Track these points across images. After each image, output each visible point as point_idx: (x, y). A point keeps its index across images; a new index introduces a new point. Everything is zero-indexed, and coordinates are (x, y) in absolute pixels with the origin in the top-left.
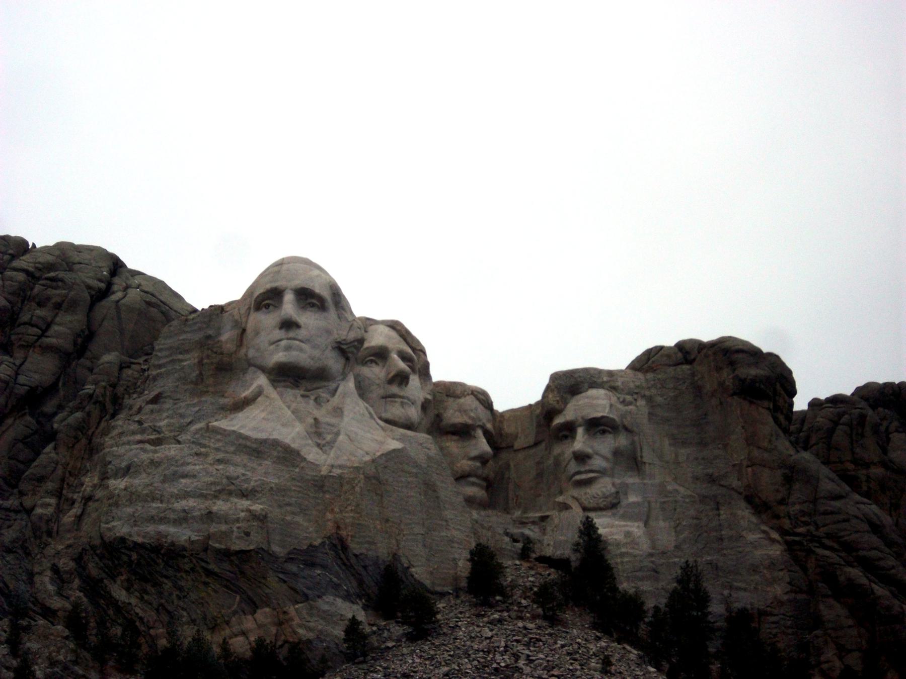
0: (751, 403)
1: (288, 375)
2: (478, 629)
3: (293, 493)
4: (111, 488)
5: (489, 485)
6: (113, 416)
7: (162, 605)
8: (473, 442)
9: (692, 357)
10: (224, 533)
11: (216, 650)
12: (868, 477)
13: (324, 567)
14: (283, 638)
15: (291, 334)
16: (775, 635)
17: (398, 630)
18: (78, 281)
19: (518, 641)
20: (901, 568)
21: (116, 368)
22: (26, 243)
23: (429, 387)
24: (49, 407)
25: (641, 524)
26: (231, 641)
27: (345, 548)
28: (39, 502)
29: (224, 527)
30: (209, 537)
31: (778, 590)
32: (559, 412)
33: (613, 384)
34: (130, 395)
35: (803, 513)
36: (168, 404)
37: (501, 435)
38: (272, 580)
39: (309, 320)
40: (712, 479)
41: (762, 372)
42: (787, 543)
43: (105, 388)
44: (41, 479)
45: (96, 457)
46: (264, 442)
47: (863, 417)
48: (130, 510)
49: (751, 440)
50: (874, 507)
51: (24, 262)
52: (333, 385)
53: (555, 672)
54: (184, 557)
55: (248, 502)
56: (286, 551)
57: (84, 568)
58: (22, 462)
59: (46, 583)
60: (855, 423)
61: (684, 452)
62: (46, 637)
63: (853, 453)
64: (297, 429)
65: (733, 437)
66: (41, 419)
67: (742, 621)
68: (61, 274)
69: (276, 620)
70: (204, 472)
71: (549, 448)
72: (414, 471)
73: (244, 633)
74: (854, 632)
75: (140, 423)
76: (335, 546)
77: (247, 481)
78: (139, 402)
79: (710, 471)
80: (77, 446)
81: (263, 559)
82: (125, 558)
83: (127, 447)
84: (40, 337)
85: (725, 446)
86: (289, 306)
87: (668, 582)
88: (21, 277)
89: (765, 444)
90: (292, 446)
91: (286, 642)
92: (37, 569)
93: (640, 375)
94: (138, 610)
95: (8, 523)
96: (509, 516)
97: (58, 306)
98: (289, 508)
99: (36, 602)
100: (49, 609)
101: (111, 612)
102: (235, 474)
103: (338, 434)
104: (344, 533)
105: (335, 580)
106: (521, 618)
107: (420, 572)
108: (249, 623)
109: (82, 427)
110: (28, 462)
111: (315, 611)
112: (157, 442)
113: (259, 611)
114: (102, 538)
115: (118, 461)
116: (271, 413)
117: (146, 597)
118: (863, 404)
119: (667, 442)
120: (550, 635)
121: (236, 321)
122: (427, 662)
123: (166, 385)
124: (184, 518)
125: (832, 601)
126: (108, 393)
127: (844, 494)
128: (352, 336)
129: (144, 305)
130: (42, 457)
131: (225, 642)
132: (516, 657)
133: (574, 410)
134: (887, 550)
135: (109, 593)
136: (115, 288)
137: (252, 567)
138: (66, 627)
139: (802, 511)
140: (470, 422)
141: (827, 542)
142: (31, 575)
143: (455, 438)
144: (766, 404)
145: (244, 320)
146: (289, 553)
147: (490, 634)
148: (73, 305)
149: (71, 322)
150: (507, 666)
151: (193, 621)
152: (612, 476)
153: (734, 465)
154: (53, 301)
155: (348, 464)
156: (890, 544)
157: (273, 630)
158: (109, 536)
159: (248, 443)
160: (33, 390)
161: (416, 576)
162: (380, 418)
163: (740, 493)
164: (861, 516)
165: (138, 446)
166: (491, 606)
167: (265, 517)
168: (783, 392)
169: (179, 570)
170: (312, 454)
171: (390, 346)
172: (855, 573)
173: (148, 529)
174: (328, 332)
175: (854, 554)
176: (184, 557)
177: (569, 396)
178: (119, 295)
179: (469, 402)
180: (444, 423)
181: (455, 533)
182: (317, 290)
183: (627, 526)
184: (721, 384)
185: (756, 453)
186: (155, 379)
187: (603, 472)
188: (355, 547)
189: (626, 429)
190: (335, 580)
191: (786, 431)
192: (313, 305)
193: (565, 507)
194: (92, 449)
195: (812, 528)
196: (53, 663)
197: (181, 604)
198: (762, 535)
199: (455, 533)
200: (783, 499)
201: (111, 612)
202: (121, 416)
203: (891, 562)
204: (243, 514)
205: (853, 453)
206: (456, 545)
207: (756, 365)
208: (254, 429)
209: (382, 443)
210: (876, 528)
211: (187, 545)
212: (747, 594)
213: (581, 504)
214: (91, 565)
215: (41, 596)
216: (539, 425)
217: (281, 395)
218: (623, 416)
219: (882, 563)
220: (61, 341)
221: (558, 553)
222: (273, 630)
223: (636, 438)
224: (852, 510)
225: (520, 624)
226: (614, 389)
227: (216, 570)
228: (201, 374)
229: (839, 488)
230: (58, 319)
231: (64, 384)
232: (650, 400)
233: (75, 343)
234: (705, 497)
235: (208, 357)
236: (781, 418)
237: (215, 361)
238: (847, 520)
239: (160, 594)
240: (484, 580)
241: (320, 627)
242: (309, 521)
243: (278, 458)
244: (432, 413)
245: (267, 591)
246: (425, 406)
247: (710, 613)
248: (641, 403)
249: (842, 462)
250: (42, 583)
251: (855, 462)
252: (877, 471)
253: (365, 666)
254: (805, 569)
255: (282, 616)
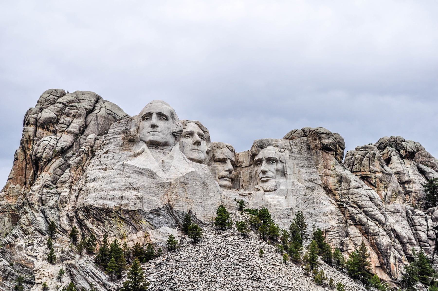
0: (326, 153)
1: (153, 144)
2: (217, 239)
3: (153, 189)
4: (88, 186)
5: (232, 180)
6: (92, 158)
7: (104, 229)
8: (226, 165)
9: (307, 134)
10: (127, 204)
11: (121, 247)
12: (375, 177)
13: (163, 216)
14: (146, 242)
15: (155, 130)
16: (331, 239)
17: (188, 239)
18: (82, 107)
19: (230, 244)
20: (380, 214)
21: (93, 141)
22: (65, 92)
23: (210, 145)
24: (69, 155)
25: (284, 197)
26: (127, 243)
27: (171, 208)
28: (63, 191)
29: (127, 202)
30: (121, 205)
31: (334, 223)
32: (257, 155)
33: (276, 145)
34: (98, 150)
35: (344, 194)
36: (110, 154)
37: (237, 161)
38: (143, 221)
39: (162, 124)
40: (311, 181)
41: (331, 141)
42: (338, 205)
43: (89, 148)
44: (64, 182)
45: (84, 174)
46: (143, 169)
47: (374, 154)
48: (94, 195)
49: (326, 167)
50: (373, 191)
51: (63, 100)
52: (170, 148)
53: (242, 257)
54: (112, 212)
55: (137, 192)
56: (150, 210)
57: (78, 215)
58: (58, 175)
59: (64, 221)
60: (371, 156)
61: (302, 170)
62: (62, 242)
63: (370, 168)
64: (156, 165)
65: (320, 165)
66: (66, 159)
67: (318, 235)
68: (75, 104)
69: (144, 236)
70: (122, 181)
71: (254, 167)
72: (199, 179)
73: (132, 240)
74: (361, 238)
75: (100, 162)
76: (168, 208)
77: (137, 184)
78: (101, 153)
79: (311, 177)
80: (78, 170)
81: (140, 213)
82: (92, 213)
83: (95, 171)
84: (67, 128)
85: (317, 168)
86: (154, 120)
87: (292, 219)
88: (61, 105)
89: (331, 168)
90: (154, 171)
91: (148, 243)
92: (61, 216)
93: (287, 141)
94: (96, 231)
95: (52, 198)
96: (238, 192)
97: (74, 116)
98: (151, 194)
99: (61, 227)
100: (65, 230)
101: (86, 232)
102: (132, 182)
103: (170, 166)
104: (171, 203)
105: (167, 220)
106: (233, 235)
107: (200, 217)
108: (134, 236)
109: (79, 163)
110: (60, 175)
111: (158, 232)
112: (105, 169)
113: (138, 232)
114: (84, 205)
115: (91, 176)
116: (147, 158)
117: (99, 227)
118: (375, 149)
119: (296, 166)
120: (243, 242)
121: (136, 124)
122: (197, 253)
123: (111, 147)
124: (113, 198)
125: (353, 227)
126: (90, 150)
127: (361, 186)
128: (177, 130)
129: (107, 115)
130: (65, 175)
131: (125, 243)
132: (229, 250)
133: (262, 154)
134: (375, 207)
135: (86, 225)
136: (96, 108)
137: (136, 216)
138: (69, 238)
139: (344, 193)
140: (225, 157)
141: (353, 205)
142: (59, 217)
143: (220, 163)
144: (332, 153)
145: (139, 123)
146: (150, 211)
147: (220, 242)
148: (80, 116)
149: (78, 122)
150: (224, 254)
151: (115, 236)
152: (275, 179)
153: (320, 175)
154: (72, 114)
155: (174, 178)
156: (377, 205)
157: (143, 239)
158: (86, 204)
159: (138, 170)
160: (63, 148)
161: (198, 218)
162: (190, 159)
163: (322, 186)
164: (366, 195)
165: (100, 170)
166: (223, 230)
167: (142, 198)
168: (339, 148)
169: (110, 217)
170: (160, 174)
171: (195, 131)
172: (362, 217)
173: (100, 202)
174: (169, 128)
175: (363, 209)
176: (112, 212)
177: (260, 149)
178: (98, 111)
179: (226, 150)
180: (216, 158)
181: (214, 202)
182: (165, 113)
183: (278, 198)
184: (316, 145)
185: (328, 171)
186: (107, 144)
187: (272, 178)
188: (175, 208)
189: (281, 161)
190: (167, 220)
191: (340, 162)
192: (163, 119)
193: (258, 190)
194: (84, 171)
195: (347, 199)
196: (63, 252)
197: (111, 229)
198: (330, 202)
199: (214, 202)
200: (337, 188)
201: (86, 232)
202: (94, 158)
203: (376, 212)
204: (134, 197)
205: (370, 168)
206: (214, 206)
207: (329, 138)
208: (140, 164)
209: (187, 169)
210: (371, 199)
211: (113, 208)
212: (322, 224)
213: (263, 189)
214: (80, 214)
215: (62, 225)
216: (251, 159)
217: (151, 151)
218: (280, 157)
219: (373, 213)
220: (74, 129)
221: (254, 207)
222: (143, 239)
223: (284, 165)
224: (363, 192)
225: (232, 238)
226: (277, 146)
227: (124, 217)
228: (123, 143)
229: (358, 184)
230: (74, 121)
231: (76, 145)
232: (291, 150)
233: (80, 130)
234: (308, 187)
235: (126, 136)
236: (339, 157)
237: (129, 138)
238: (361, 197)
239: (104, 226)
240: (221, 221)
241: (160, 238)
242: (158, 199)
243: (148, 175)
244: (211, 155)
245: (141, 225)
246: (208, 153)
247: (306, 232)
248: (287, 152)
249: (365, 171)
250: (63, 220)
251: (370, 172)
252: (379, 175)
253: (174, 253)
254: (344, 215)
255: (146, 234)
